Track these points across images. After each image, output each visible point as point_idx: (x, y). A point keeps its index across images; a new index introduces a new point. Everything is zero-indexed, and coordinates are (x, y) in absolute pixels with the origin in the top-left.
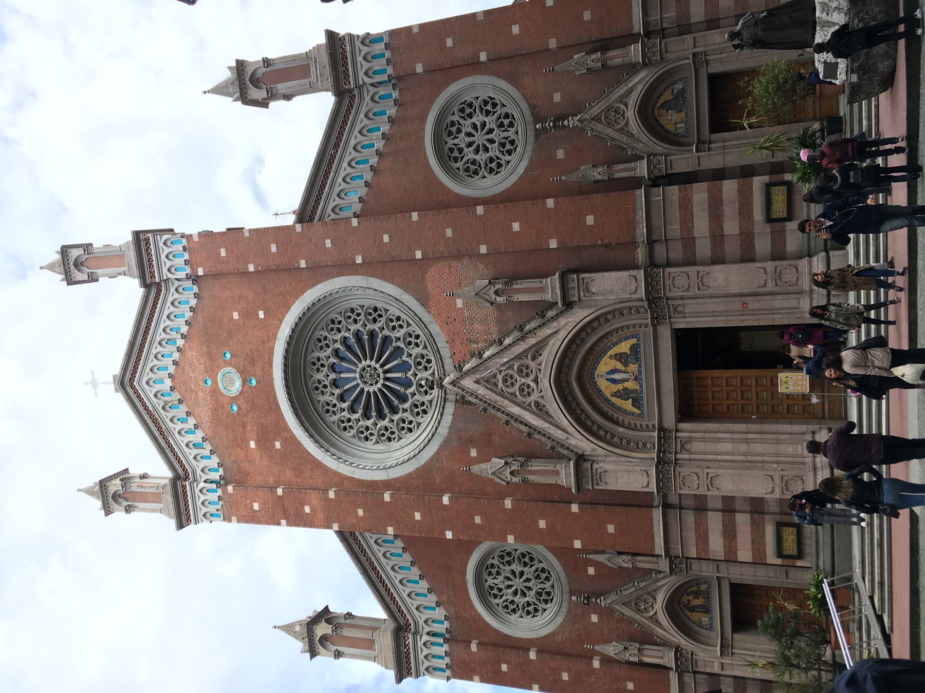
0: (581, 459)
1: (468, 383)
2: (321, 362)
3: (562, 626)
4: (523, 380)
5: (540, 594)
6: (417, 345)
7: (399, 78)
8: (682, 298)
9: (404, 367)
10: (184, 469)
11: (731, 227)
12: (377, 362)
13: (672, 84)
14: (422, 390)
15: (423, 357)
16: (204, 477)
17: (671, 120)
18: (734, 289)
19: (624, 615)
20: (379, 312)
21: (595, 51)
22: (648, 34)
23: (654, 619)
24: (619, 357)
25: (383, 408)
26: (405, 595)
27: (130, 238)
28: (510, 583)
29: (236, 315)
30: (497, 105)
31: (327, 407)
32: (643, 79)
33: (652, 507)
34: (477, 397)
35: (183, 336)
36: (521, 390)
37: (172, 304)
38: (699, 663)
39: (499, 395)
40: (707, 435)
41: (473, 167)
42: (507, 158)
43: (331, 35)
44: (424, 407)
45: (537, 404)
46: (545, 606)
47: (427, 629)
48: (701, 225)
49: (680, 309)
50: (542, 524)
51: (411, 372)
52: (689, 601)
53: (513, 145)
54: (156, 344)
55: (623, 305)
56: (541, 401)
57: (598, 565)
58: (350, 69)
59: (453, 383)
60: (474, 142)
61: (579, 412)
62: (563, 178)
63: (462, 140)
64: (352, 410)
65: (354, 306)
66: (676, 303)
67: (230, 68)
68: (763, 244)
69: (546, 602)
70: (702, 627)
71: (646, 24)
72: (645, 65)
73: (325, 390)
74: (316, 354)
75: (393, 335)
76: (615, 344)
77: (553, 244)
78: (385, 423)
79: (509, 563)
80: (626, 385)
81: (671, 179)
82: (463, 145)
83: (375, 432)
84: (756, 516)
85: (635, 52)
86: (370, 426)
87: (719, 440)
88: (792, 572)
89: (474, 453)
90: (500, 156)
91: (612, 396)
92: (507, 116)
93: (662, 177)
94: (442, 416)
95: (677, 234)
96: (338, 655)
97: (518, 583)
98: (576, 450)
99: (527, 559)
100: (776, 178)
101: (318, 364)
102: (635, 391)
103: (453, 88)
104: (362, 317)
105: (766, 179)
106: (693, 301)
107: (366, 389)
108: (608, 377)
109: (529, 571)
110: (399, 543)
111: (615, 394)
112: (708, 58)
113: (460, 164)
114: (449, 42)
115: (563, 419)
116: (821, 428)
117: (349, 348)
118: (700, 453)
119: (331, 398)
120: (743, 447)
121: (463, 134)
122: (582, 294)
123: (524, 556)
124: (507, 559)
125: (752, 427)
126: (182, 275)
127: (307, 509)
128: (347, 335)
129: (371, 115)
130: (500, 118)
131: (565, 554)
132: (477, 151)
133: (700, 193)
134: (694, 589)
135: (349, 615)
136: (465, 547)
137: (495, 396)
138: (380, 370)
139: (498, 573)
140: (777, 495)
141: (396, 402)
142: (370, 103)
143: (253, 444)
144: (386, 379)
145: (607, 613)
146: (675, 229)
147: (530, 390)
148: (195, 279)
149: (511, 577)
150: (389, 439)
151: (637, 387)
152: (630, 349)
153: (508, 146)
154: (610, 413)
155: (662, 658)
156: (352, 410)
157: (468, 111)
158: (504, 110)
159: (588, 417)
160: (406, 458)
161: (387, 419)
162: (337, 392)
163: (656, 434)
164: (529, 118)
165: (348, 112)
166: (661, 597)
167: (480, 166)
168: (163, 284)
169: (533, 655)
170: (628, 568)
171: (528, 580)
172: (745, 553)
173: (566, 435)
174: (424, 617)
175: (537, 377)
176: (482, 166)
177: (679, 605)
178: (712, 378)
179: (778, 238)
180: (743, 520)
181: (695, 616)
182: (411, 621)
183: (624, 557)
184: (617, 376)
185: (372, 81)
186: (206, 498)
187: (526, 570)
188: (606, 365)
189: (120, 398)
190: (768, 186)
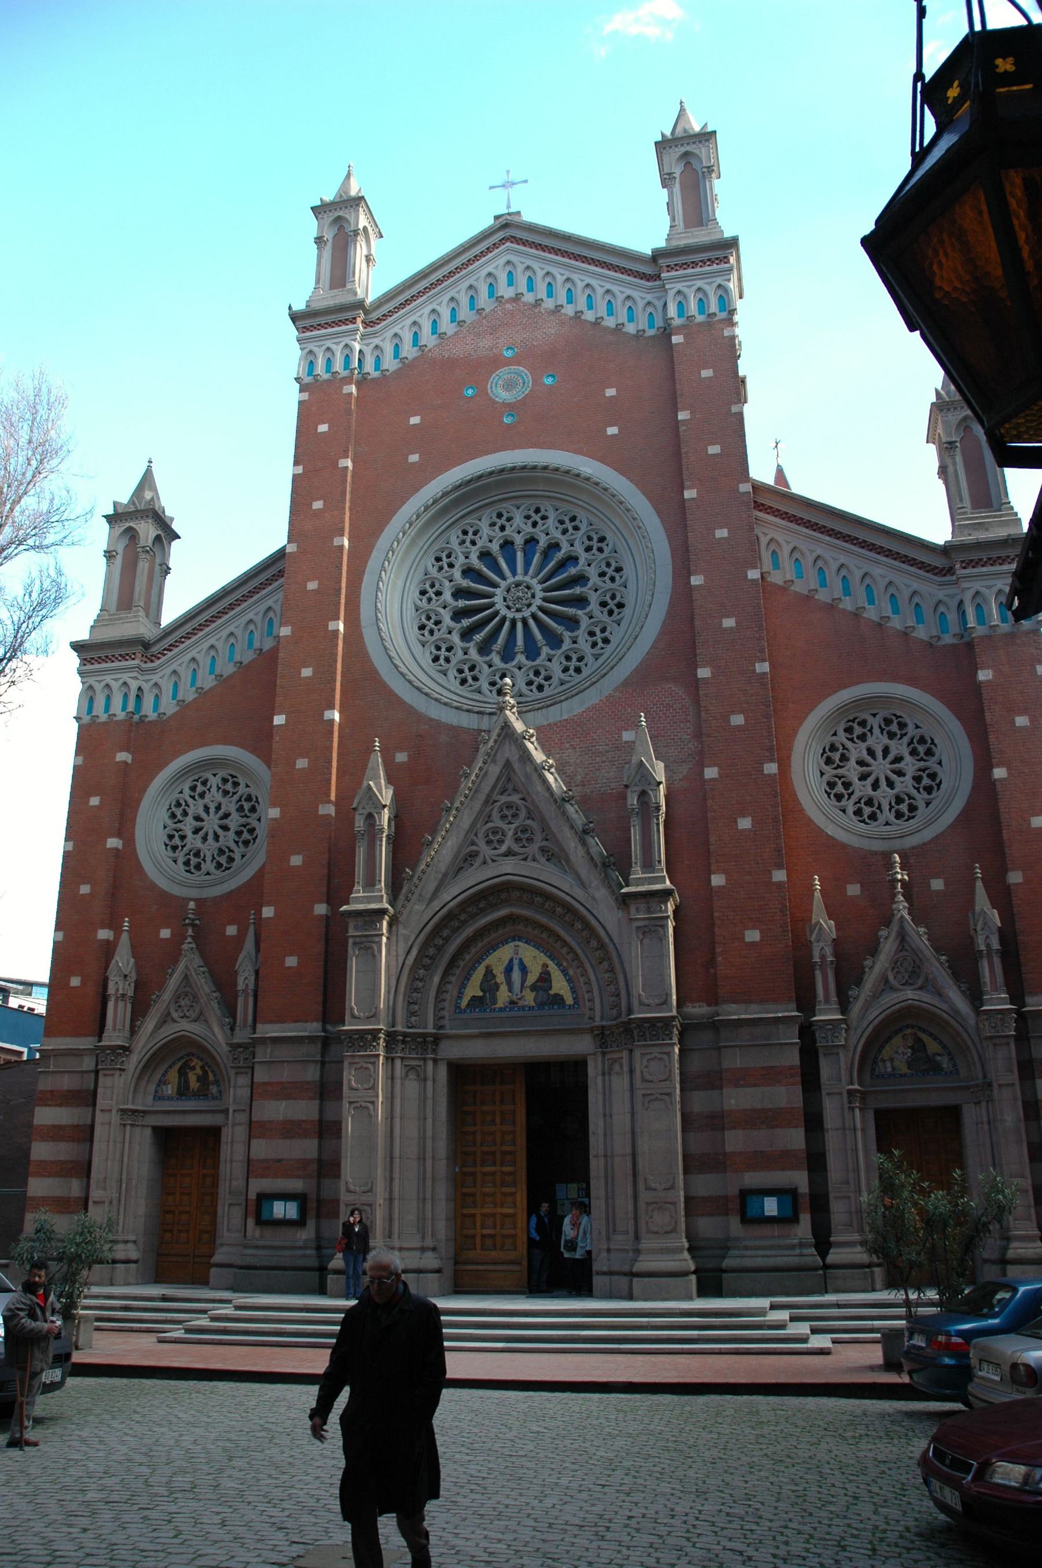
3: (153, 886)
4: (510, 833)
5: (197, 854)
6: (566, 670)
7: (970, 646)
8: (631, 1071)
10: (380, 320)
11: (735, 1141)
12: (541, 609)
13: (949, 1054)
15: (548, 678)
16: (368, 351)
18: (644, 1145)
19: (171, 975)
20: (616, 611)
21: (1002, 941)
23: (166, 1018)
24: (545, 978)
25: (469, 617)
26: (193, 653)
27: (728, 234)
28: (212, 810)
29: (611, 392)
30: (929, 793)
32: (957, 1011)
33: (325, 1022)
35: (579, 314)
36: (495, 832)
37: (629, 297)
38: (109, 1079)
39: (489, 796)
40: (429, 1102)
41: (836, 756)
42: (851, 810)
44: (470, 681)
45: (473, 855)
46: (180, 861)
47: (146, 687)
48: (737, 1099)
49: (617, 1067)
50: (296, 860)
52: (194, 1068)
53: (869, 817)
54: (567, 274)
55: (622, 984)
56: (479, 860)
57: (239, 941)
58: (984, 569)
61: (463, 917)
64: (468, 572)
65: (628, 571)
66: (625, 1062)
68: (707, 1185)
69: (187, 863)
70: (158, 1085)
73: (497, 528)
74: (552, 516)
75: (581, 633)
76: (565, 972)
79: (241, 809)
80: (504, 988)
81: (809, 1053)
82: (870, 741)
84: (314, 1166)
85: (998, 1001)
86: (442, 598)
88: (237, 1213)
90: (854, 798)
91: (487, 967)
92: (912, 808)
93: (814, 1041)
94: (457, 708)
95: (727, 1064)
96: (109, 555)
97: (212, 823)
99: (246, 836)
101: (536, 518)
102: (494, 1001)
104: (609, 585)
105: (804, 1188)
106: (627, 1086)
107: (498, 591)
108: (516, 962)
109: (228, 839)
110: (268, 644)
112: (984, 1104)
113: (842, 736)
116: (441, 1259)
117: (562, 565)
118: (402, 1092)
119: (485, 538)
123: (252, 831)
124: (247, 806)
125: (442, 1166)
127: (318, 505)
128: (582, 561)
130: (910, 798)
131: (253, 893)
132: (861, 763)
133: (787, 1096)
134: (211, 1077)
135: (167, 571)
136: (261, 740)
138: (527, 613)
139: (226, 793)
143: (415, 420)
144: (514, 623)
145: (172, 953)
146: (734, 1060)
147: (495, 844)
148: (667, 332)
149: (221, 813)
150: (422, 627)
151: (500, 1004)
152: (557, 995)
153: (867, 811)
155: (114, 1029)
157: (921, 749)
158: (921, 805)
159: (455, 931)
161: (452, 624)
162: (495, 547)
163: (430, 1030)
165: (922, 566)
166: (195, 1029)
167: (839, 767)
168: (657, 283)
170: (235, 984)
171: (217, 837)
172: (261, 1149)
173: (428, 896)
175: (515, 854)
176: (840, 771)
177: (188, 1055)
179: (718, 1206)
181: (173, 1075)
182: (158, 662)
183: (253, 978)
184: (516, 975)
187: (231, 835)
188: (534, 958)
189: (487, 222)
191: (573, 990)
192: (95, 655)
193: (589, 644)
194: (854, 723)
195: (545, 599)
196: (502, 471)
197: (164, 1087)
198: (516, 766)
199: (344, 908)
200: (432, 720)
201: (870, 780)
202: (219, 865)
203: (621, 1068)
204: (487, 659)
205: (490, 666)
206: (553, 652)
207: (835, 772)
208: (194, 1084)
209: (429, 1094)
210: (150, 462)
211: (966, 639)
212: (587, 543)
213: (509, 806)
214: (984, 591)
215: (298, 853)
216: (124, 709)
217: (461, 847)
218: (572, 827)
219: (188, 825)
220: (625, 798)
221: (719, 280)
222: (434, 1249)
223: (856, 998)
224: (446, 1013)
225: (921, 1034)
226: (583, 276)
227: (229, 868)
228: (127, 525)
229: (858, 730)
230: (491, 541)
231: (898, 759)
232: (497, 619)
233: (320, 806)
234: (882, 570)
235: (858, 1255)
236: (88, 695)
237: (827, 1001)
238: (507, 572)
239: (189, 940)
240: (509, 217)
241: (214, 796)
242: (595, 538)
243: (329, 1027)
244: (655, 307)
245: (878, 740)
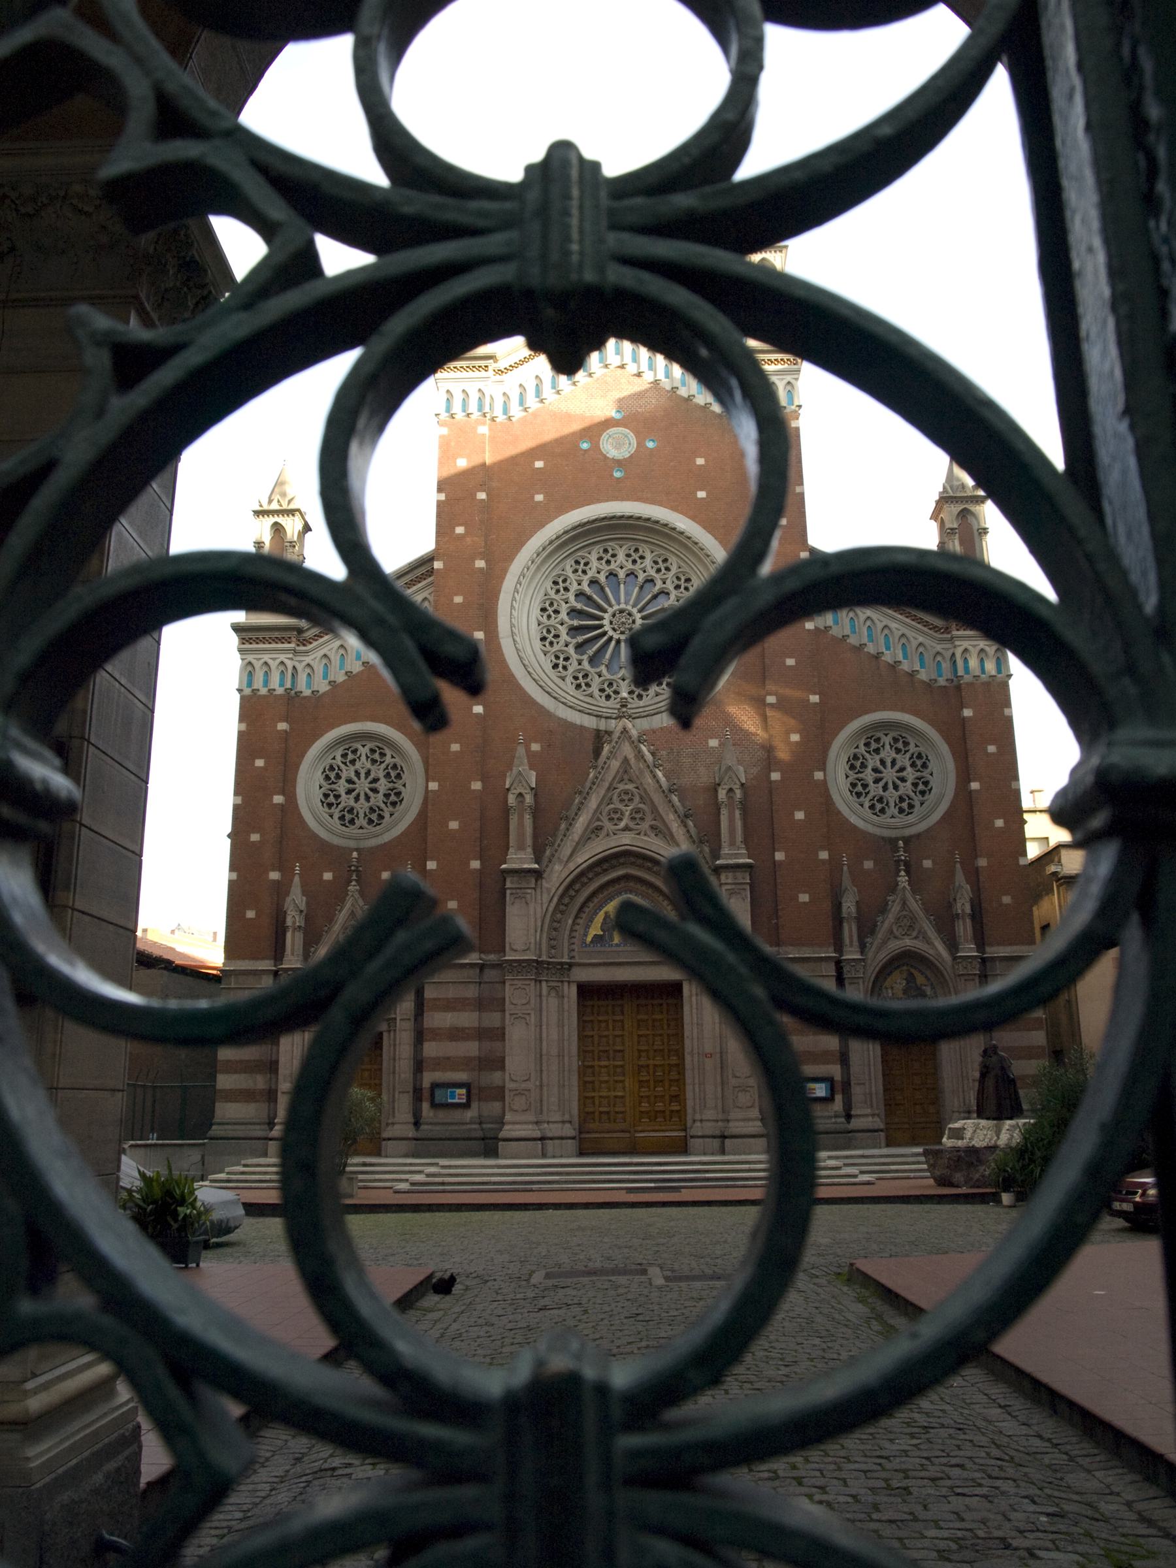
0: (538, 875)
1: (627, 750)
2: (639, 561)
3: (315, 836)
4: (627, 813)
14: (605, 686)
17: (897, 982)
19: (340, 911)
22: (984, 961)
28: (363, 776)
29: (700, 461)
31: (582, 562)
34: (608, 758)
36: (615, 811)
39: (611, 784)
41: (858, 764)
42: (867, 805)
44: (584, 687)
45: (599, 828)
46: (336, 816)
47: (300, 667)
50: (454, 825)
56: (604, 833)
59: (625, 731)
60: (885, 767)
62: (845, 868)
63: (888, 754)
64: (580, 595)
69: (342, 818)
71: (993, 959)
72: (955, 958)
73: (603, 562)
77: (779, 856)
78: (564, 636)
79: (388, 775)
82: (882, 755)
83: (552, 622)
85: (969, 949)
87: (560, 1024)
89: (535, 747)
90: (870, 796)
91: (606, 913)
92: (911, 806)
97: (363, 786)
98: (548, 869)
99: (395, 798)
100: (838, 1087)
101: (635, 556)
103: (944, 748)
107: (606, 616)
109: (378, 800)
114: (992, 749)
115: (584, 858)
117: (655, 597)
119: (594, 570)
120: (554, 1051)
121: (894, 755)
122: (729, 887)
123: (398, 794)
124: (393, 774)
127: (460, 530)
129: (921, 649)
132: (875, 770)
137: (610, 779)
139: (374, 761)
140: (509, 1085)
142: (934, 651)
150: (543, 639)
153: (879, 806)
154: (587, 910)
155: (293, 954)
156: (580, 595)
157: (919, 763)
158: (917, 804)
159: (584, 885)
160: (526, 663)
161: (569, 639)
163: (566, 960)
164: (907, 832)
167: (859, 772)
169: (278, 799)
171: (368, 798)
174: (315, 665)
175: (630, 830)
176: (860, 775)
178: (622, 1021)
180: (471, 1048)
182: (310, 647)
187: (380, 796)
192: (254, 635)
194: (871, 737)
196: (613, 517)
198: (632, 761)
199: (504, 866)
200: (559, 718)
202: (371, 821)
209: (566, 1007)
211: (955, 683)
212: (676, 582)
213: (626, 792)
214: (970, 648)
215: (455, 820)
216: (281, 685)
217: (590, 822)
218: (676, 812)
220: (716, 791)
221: (789, 378)
222: (570, 1122)
223: (871, 944)
224: (575, 947)
225: (913, 970)
235: (878, 1123)
236: (249, 670)
237: (851, 945)
238: (613, 601)
239: (354, 883)
241: (363, 764)
242: (683, 579)
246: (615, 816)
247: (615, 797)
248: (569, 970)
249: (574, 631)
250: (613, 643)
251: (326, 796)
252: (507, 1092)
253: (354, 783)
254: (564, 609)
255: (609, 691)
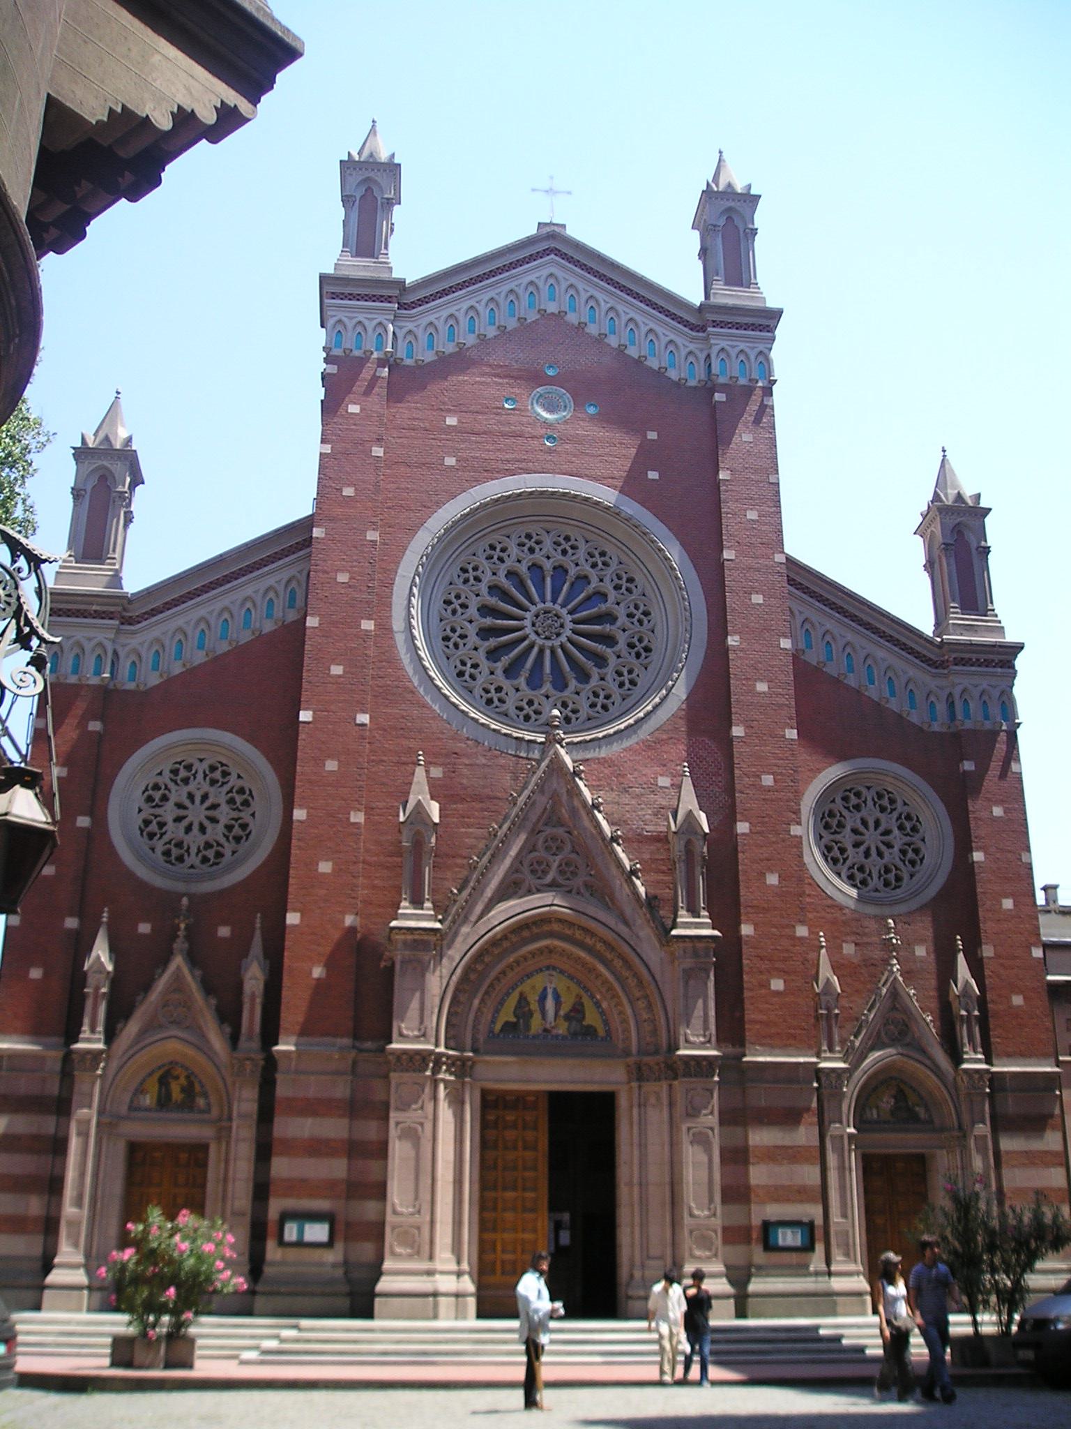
3: (131, 875)
4: (556, 864)
6: (593, 705)
9: (561, 684)
16: (400, 335)
19: (160, 976)
20: (644, 654)
24: (577, 1011)
27: (771, 303)
33: (356, 1037)
39: (535, 824)
41: (834, 822)
43: (1019, 647)
49: (653, 1100)
51: (552, 692)
52: (177, 1078)
57: (240, 947)
60: (867, 828)
64: (494, 589)
65: (656, 614)
66: (664, 1095)
67: (978, 497)
70: (134, 1094)
73: (526, 549)
75: (610, 671)
76: (598, 1004)
78: (473, 639)
79: (231, 801)
80: (537, 1017)
82: (864, 813)
89: (437, 772)
90: (848, 863)
91: (521, 994)
92: (898, 879)
96: (77, 493)
97: (197, 814)
99: (240, 833)
100: (819, 1233)
102: (528, 1027)
105: (819, 1221)
107: (528, 615)
108: (550, 991)
109: (216, 832)
111: (523, 999)
117: (588, 598)
119: (514, 557)
123: (244, 826)
124: (239, 799)
126: (716, 368)
128: (611, 599)
134: (197, 1088)
141: (506, 660)
148: (709, 388)
149: (207, 804)
150: (447, 639)
157: (908, 825)
158: (906, 876)
167: (836, 832)
171: (203, 829)
180: (337, 1168)
184: (550, 1004)
185: (957, 697)
186: (370, 330)
187: (220, 828)
190: (810, 1226)
191: (606, 1023)
193: (617, 683)
195: (574, 632)
197: (141, 1097)
198: (565, 798)
199: (394, 924)
201: (862, 848)
203: (659, 1098)
204: (516, 682)
205: (517, 690)
206: (582, 686)
207: (832, 837)
208: (177, 1094)
210: (118, 393)
212: (616, 581)
213: (554, 839)
219: (169, 812)
221: (761, 347)
226: (628, 309)
227: (217, 864)
228: (100, 463)
229: (854, 800)
230: (519, 561)
231: (887, 832)
232: (526, 643)
233: (352, 813)
234: (883, 654)
240: (556, 229)
241: (199, 786)
243: (357, 1044)
244: (696, 358)
245: (870, 813)
246: (539, 869)
247: (540, 842)
248: (472, 1067)
249: (485, 633)
250: (536, 650)
251: (147, 823)
252: (388, 1230)
253: (185, 808)
254: (474, 604)
255: (528, 710)
